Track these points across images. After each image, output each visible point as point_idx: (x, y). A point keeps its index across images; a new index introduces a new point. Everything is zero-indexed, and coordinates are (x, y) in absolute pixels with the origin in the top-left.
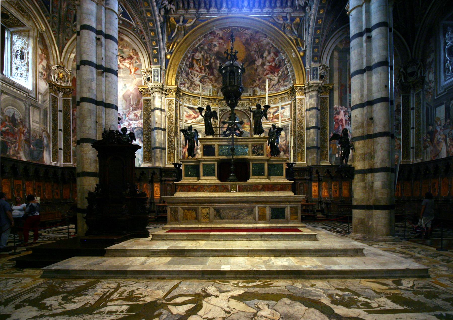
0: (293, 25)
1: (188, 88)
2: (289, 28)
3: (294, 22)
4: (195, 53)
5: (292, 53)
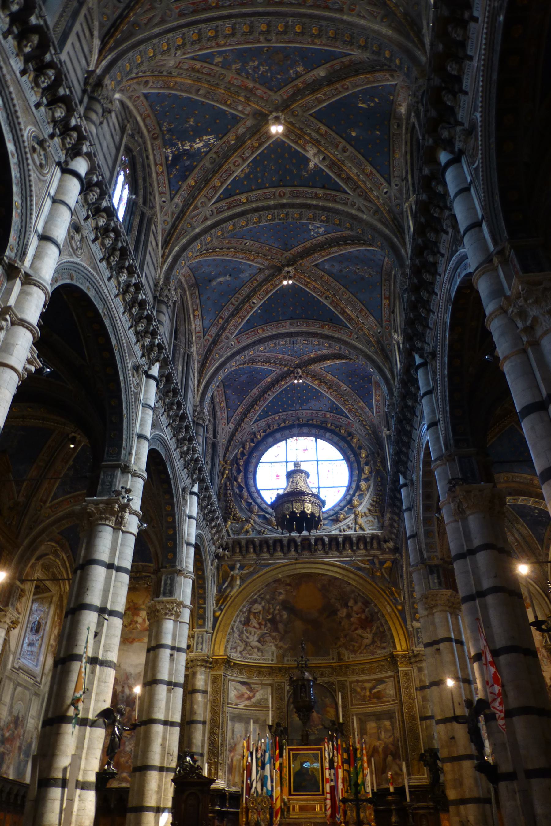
0: (383, 570)
1: (241, 652)
2: (378, 574)
3: (385, 566)
4: (253, 605)
5: (385, 608)
